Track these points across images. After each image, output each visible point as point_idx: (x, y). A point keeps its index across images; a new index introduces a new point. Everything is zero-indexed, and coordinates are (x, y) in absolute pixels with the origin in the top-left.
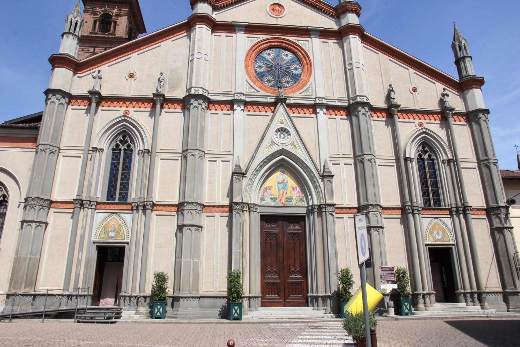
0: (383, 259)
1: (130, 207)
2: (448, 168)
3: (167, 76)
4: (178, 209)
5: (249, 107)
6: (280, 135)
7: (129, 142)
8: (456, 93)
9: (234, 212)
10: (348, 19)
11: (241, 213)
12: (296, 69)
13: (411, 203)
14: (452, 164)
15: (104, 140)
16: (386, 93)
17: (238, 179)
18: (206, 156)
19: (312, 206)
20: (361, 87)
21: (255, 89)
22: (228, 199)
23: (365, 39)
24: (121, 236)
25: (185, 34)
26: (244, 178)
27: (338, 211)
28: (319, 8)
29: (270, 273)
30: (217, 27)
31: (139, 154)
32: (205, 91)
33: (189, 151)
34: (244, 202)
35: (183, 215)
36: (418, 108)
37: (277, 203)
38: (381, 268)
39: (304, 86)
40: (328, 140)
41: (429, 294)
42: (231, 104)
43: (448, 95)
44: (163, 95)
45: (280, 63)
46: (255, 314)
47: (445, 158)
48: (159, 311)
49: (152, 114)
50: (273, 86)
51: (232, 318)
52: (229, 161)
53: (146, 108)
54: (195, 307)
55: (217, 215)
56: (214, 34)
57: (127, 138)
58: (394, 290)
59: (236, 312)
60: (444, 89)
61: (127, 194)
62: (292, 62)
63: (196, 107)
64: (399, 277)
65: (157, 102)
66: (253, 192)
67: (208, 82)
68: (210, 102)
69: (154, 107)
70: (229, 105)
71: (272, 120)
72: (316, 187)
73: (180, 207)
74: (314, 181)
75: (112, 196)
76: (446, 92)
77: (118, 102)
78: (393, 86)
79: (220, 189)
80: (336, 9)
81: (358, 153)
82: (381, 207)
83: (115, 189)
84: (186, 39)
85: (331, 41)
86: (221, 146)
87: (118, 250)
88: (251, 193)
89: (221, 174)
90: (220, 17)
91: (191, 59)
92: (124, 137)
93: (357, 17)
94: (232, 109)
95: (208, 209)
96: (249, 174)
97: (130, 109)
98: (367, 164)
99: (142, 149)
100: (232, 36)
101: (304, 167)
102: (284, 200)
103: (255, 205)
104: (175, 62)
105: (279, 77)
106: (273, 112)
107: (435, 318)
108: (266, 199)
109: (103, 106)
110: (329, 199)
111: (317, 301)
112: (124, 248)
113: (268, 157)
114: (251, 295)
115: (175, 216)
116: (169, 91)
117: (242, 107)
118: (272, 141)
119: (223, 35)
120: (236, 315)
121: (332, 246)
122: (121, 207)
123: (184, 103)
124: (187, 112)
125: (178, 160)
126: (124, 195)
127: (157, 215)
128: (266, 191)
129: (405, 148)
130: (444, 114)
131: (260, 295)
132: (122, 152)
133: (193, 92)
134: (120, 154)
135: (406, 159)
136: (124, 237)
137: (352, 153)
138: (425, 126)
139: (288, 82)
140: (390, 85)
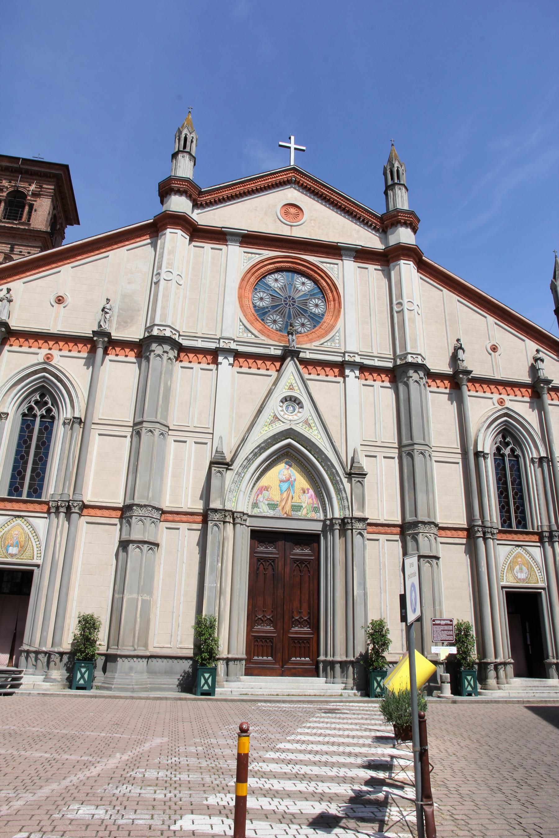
0: (437, 607)
1: (45, 508)
2: (539, 471)
3: (115, 304)
4: (122, 514)
5: (241, 360)
6: (287, 407)
7: (50, 405)
8: (555, 357)
9: (210, 524)
10: (399, 235)
11: (221, 525)
12: (317, 306)
13: (483, 522)
14: (545, 465)
15: (10, 400)
16: (452, 350)
17: (219, 472)
18: (170, 433)
19: (331, 520)
20: (414, 340)
21: (252, 334)
22: (202, 502)
23: (423, 267)
24: (28, 553)
25: (149, 241)
26: (228, 471)
27: (370, 529)
28: (355, 216)
29: (261, 621)
30: (197, 233)
31: (64, 424)
32: (174, 332)
33: (145, 424)
34: (226, 508)
35: (130, 524)
36: (498, 377)
37: (278, 513)
38: (434, 621)
39: (327, 333)
40: (361, 419)
41: (505, 664)
42: (214, 355)
43: (542, 361)
44: (109, 335)
45: (292, 295)
46: (236, 686)
47: (535, 456)
48: (82, 677)
49: (90, 362)
50: (280, 331)
51: (199, 691)
52: (206, 444)
53: (79, 352)
54: (142, 673)
55: (183, 527)
56: (194, 243)
57: (47, 398)
58: (451, 656)
59: (206, 682)
60: (538, 351)
61: (41, 487)
62: (312, 295)
63: (159, 355)
64: (460, 637)
65: (98, 344)
66: (242, 494)
67: (181, 317)
68: (181, 349)
69: (93, 351)
70: (210, 355)
71: (275, 383)
72: (338, 491)
73: (125, 512)
74: (337, 481)
75: (16, 489)
76: (541, 355)
77: (36, 341)
78: (462, 342)
79: (190, 486)
80: (381, 219)
81: (405, 442)
82: (436, 525)
83: (23, 478)
84: (149, 248)
85: (371, 267)
86: (196, 419)
87: (20, 575)
88: (237, 494)
89: (192, 463)
90: (205, 218)
91: (155, 280)
92: (42, 396)
93: (412, 234)
94: (215, 362)
95: (170, 517)
96: (236, 466)
97: (55, 353)
98: (418, 458)
99: (69, 416)
100: (221, 250)
101: (322, 458)
102: (288, 508)
103: (244, 514)
104: (129, 283)
105: (289, 317)
106: (278, 371)
107: (513, 702)
108: (261, 505)
109: (11, 345)
110: (358, 509)
111: (333, 669)
112: (32, 572)
113: (267, 439)
114: (230, 656)
115: (116, 525)
116: (117, 329)
117: (231, 360)
118: (275, 415)
119: (208, 248)
120: (206, 687)
121: (359, 584)
122: (31, 507)
123: (141, 348)
124: (144, 363)
125: (126, 437)
126: (37, 489)
127: (87, 523)
128: (261, 493)
129: (477, 436)
131: (244, 656)
132: (38, 420)
133: (155, 332)
134: (34, 422)
135: (477, 454)
136: (32, 556)
137: (396, 441)
138: (508, 404)
139: (303, 325)
140: (458, 340)
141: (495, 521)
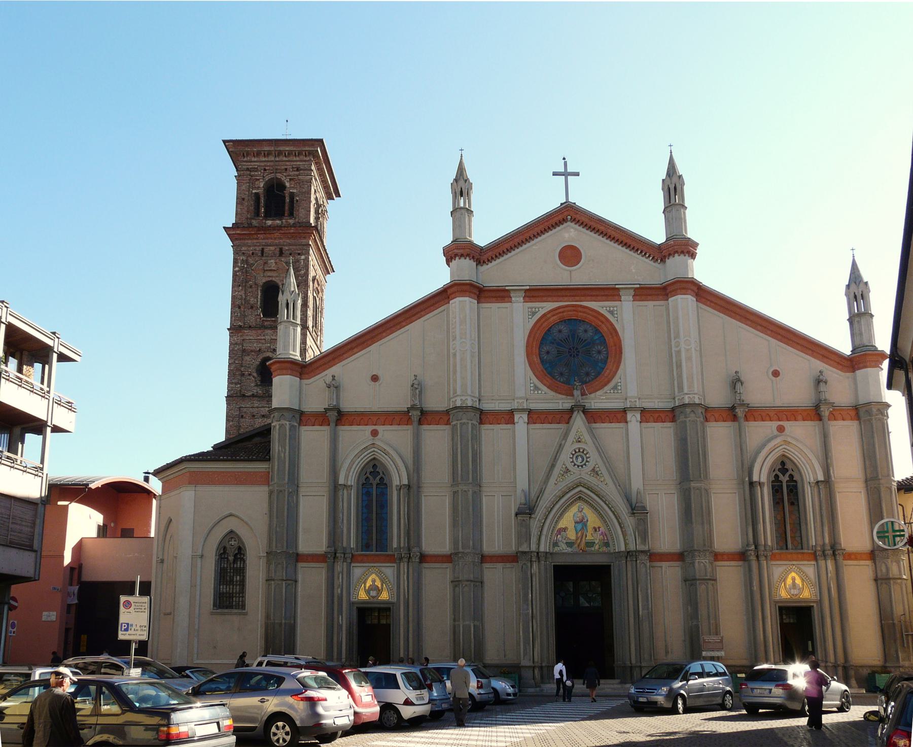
37: (575, 549)
42: (508, 417)
71: (565, 436)
102: (583, 545)
103: (546, 553)
108: (560, 544)
130: (816, 412)
141: (770, 543)
